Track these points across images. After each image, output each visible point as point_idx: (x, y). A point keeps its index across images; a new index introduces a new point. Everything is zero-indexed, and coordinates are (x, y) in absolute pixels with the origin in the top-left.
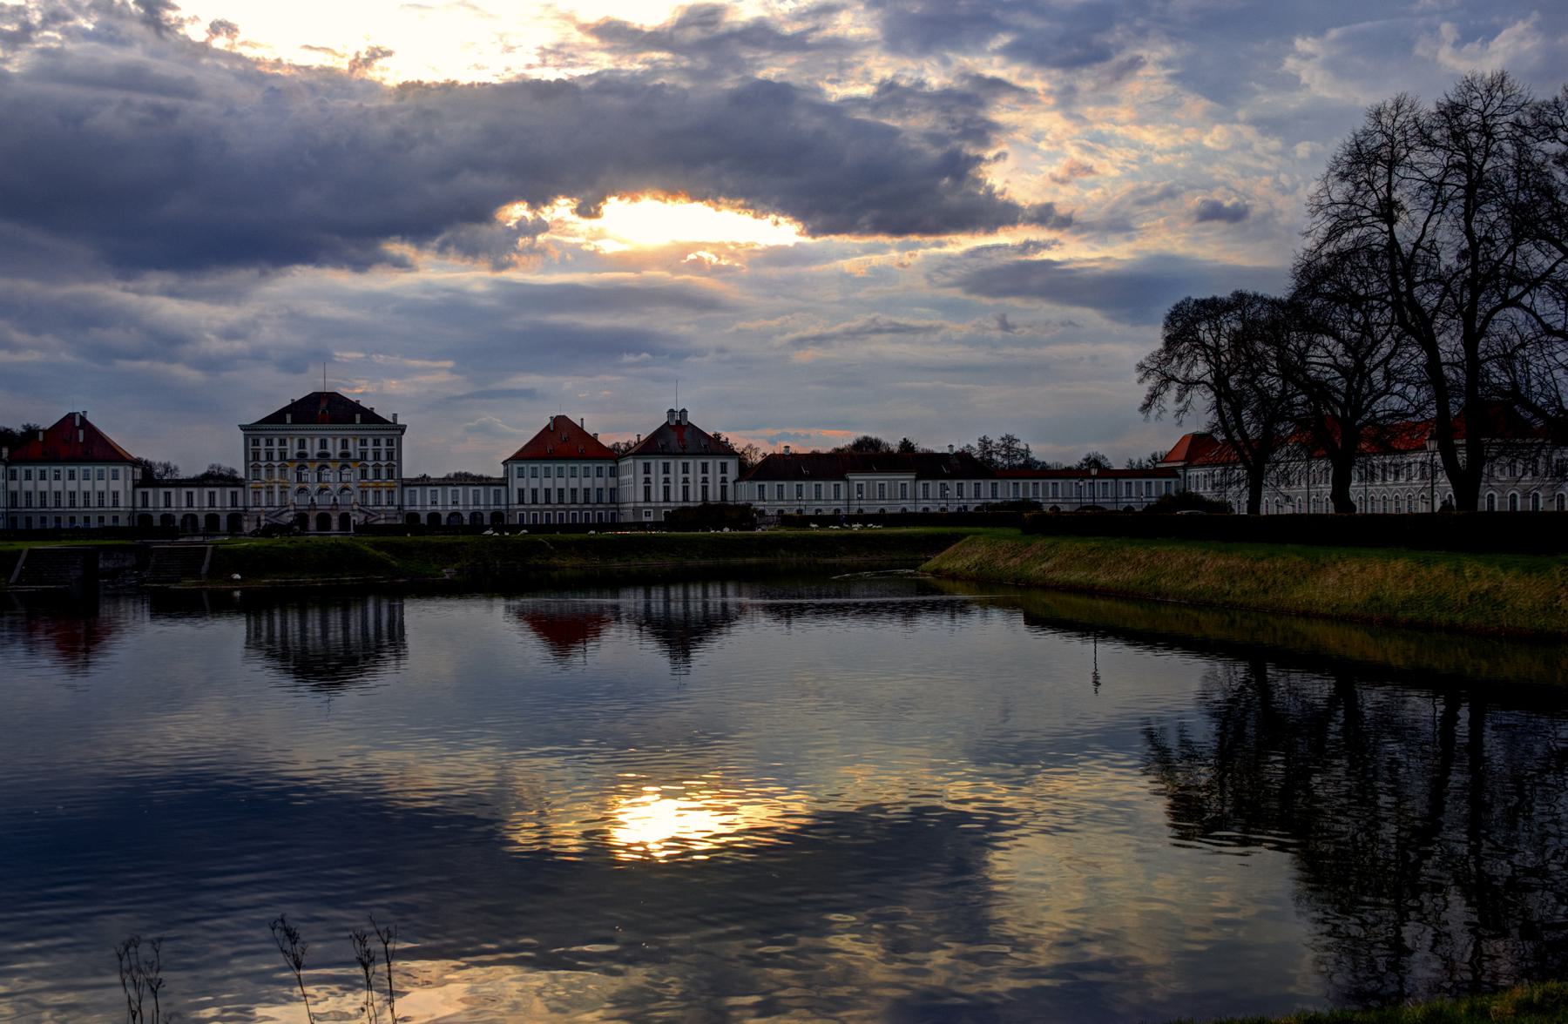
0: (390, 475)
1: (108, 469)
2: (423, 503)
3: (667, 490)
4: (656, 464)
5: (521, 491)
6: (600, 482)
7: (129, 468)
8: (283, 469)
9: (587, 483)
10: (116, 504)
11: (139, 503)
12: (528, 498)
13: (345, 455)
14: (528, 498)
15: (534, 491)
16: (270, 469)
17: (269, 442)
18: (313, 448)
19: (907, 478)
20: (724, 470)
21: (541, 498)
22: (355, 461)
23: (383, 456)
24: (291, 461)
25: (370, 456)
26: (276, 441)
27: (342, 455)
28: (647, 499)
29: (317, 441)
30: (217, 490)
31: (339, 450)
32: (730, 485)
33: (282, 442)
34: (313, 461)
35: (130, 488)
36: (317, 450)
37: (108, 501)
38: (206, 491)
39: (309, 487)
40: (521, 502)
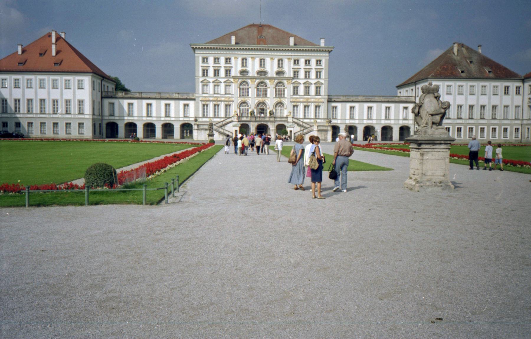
0: (318, 93)
6: (507, 100)
7: (98, 81)
8: (228, 85)
9: (495, 101)
10: (81, 112)
13: (280, 73)
16: (217, 84)
17: (217, 60)
18: (253, 67)
23: (313, 75)
25: (302, 74)
26: (222, 60)
27: (278, 73)
29: (257, 61)
31: (276, 69)
33: (228, 60)
35: (99, 99)
36: (257, 68)
37: (74, 109)
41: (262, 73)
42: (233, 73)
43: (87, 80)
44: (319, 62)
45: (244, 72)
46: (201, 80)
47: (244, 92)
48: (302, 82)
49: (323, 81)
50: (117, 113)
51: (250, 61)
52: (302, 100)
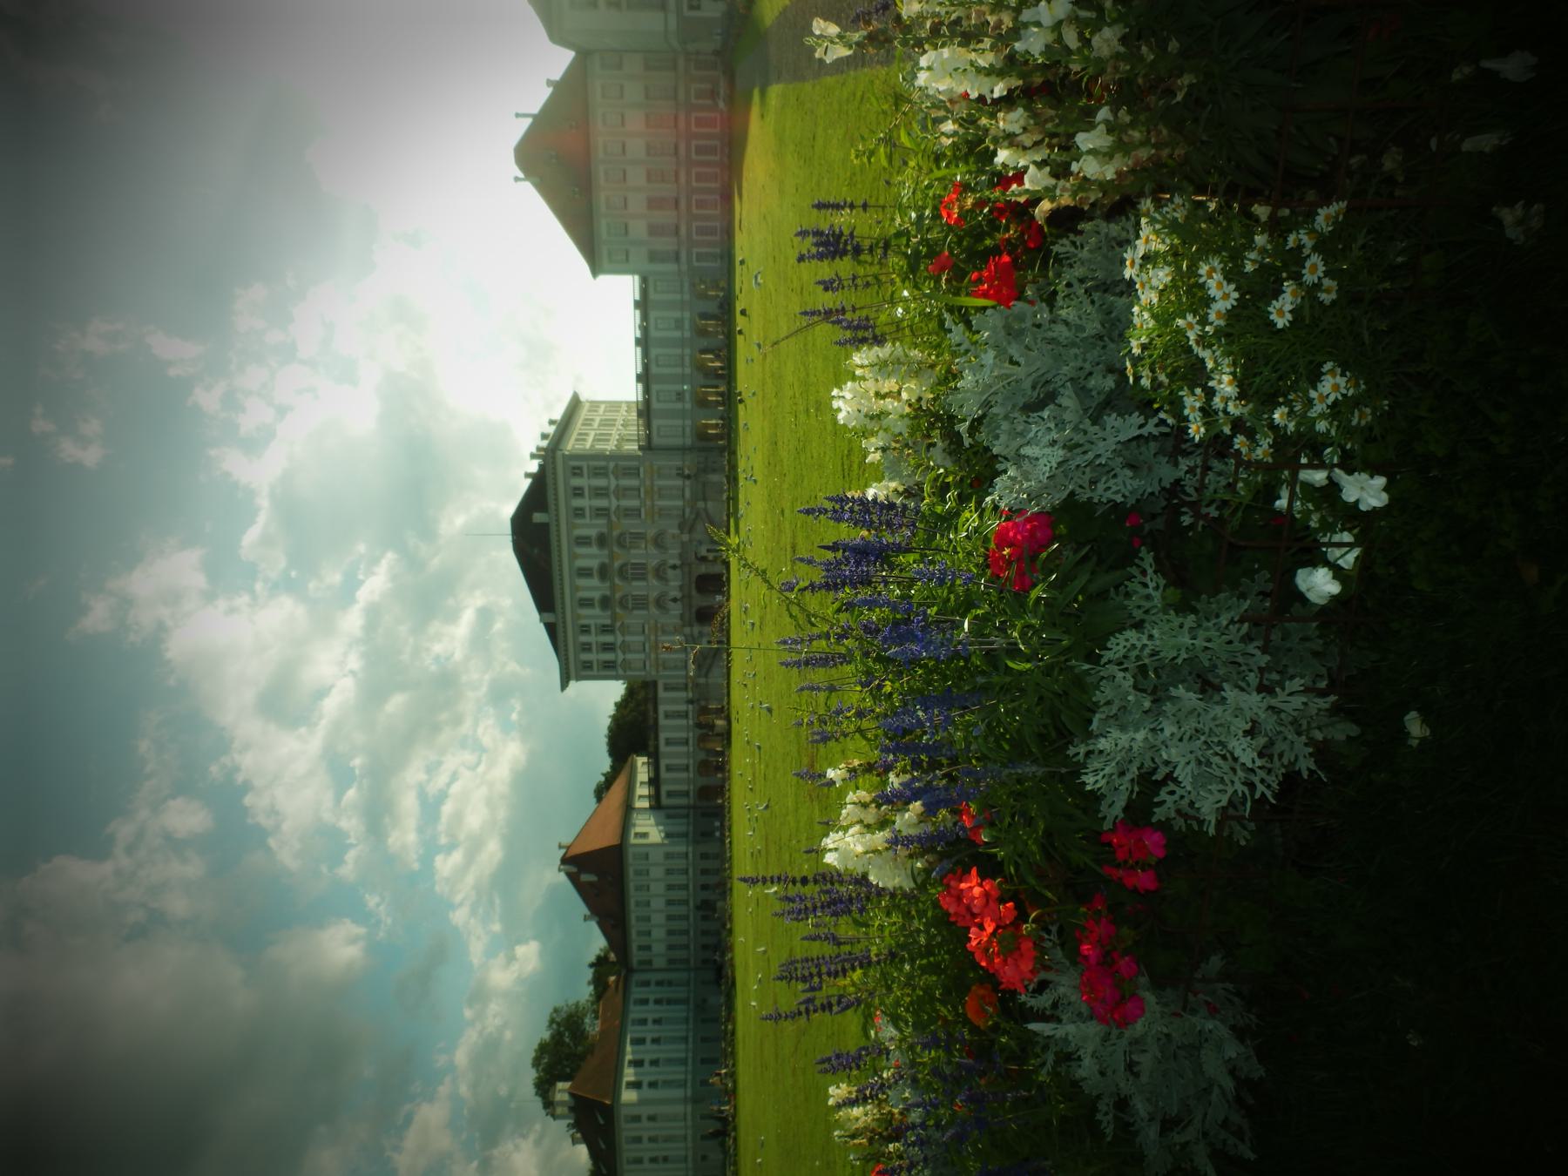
0: (633, 472)
8: (625, 630)
13: (602, 541)
17: (587, 648)
18: (593, 587)
22: (610, 524)
23: (601, 482)
24: (614, 617)
25: (601, 503)
29: (582, 582)
30: (662, 709)
31: (594, 550)
33: (585, 630)
34: (613, 588)
36: (595, 581)
38: (662, 721)
39: (654, 595)
41: (604, 572)
42: (608, 622)
44: (577, 472)
46: (621, 672)
47: (641, 603)
48: (614, 503)
49: (612, 465)
50: (685, 788)
52: (648, 503)
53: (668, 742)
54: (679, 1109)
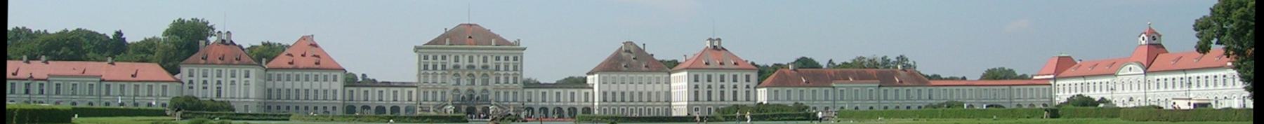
1: (330, 75)
2: (536, 98)
3: (709, 93)
4: (703, 76)
5: (605, 93)
11: (347, 98)
12: (609, 97)
13: (485, 67)
14: (609, 97)
15: (614, 94)
17: (435, 58)
18: (464, 62)
19: (873, 85)
20: (748, 80)
21: (618, 98)
22: (492, 72)
23: (511, 68)
24: (450, 71)
25: (502, 68)
26: (439, 57)
28: (697, 99)
29: (467, 57)
31: (481, 63)
32: (752, 90)
33: (444, 58)
34: (463, 71)
36: (467, 63)
40: (605, 101)
43: (340, 75)
44: (516, 59)
45: (456, 67)
51: (461, 58)
53: (366, 92)
54: (252, 94)
